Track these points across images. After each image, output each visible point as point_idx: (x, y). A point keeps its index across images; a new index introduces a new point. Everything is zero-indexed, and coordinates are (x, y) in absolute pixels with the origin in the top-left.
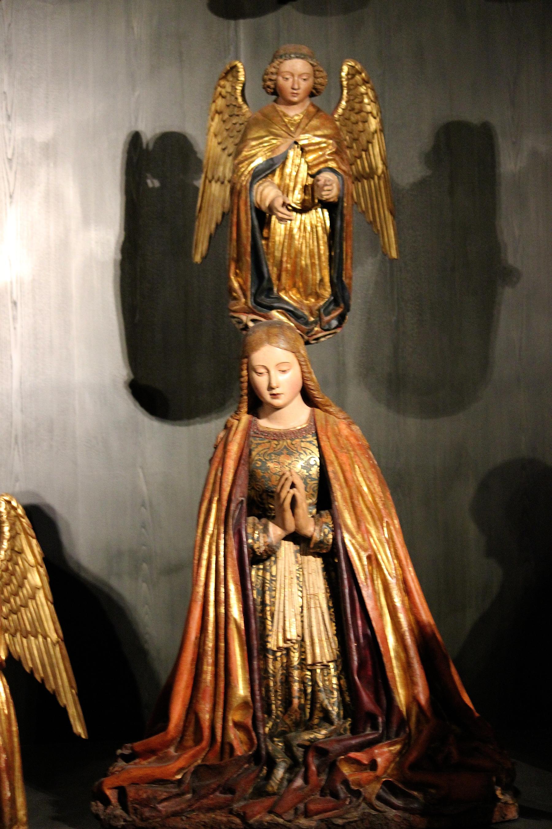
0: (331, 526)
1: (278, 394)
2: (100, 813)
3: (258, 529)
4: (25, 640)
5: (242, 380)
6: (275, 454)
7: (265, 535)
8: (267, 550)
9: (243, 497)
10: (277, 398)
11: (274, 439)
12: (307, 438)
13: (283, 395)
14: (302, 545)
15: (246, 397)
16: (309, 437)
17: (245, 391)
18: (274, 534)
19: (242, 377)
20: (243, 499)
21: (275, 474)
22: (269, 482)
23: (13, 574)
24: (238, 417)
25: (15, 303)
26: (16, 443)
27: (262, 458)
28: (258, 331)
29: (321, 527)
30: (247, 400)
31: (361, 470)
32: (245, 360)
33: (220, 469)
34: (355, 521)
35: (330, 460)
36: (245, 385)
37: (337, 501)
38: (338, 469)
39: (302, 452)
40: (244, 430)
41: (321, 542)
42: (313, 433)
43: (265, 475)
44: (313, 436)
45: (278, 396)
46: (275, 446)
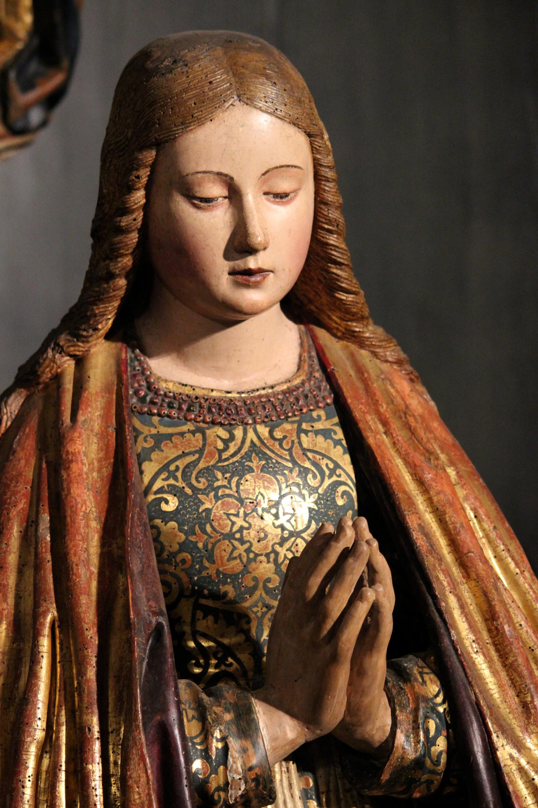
0: (441, 709)
1: (260, 271)
3: (218, 721)
5: (125, 221)
6: (224, 470)
7: (248, 744)
8: (251, 794)
9: (160, 613)
10: (256, 285)
11: (214, 423)
12: (313, 420)
13: (272, 275)
14: (321, 772)
15: (122, 282)
16: (319, 418)
17: (127, 261)
18: (274, 739)
19: (126, 211)
20: (161, 619)
21: (230, 536)
22: (207, 564)
24: (80, 348)
27: (180, 484)
28: (197, 59)
29: (416, 710)
30: (122, 293)
31: (486, 526)
32: (150, 155)
33: (45, 518)
34: (511, 693)
35: (405, 492)
36: (134, 237)
37: (456, 629)
38: (429, 518)
39: (307, 465)
40: (107, 389)
41: (419, 763)
42: (328, 404)
43: (192, 538)
44: (328, 417)
45: (257, 278)
46: (220, 445)
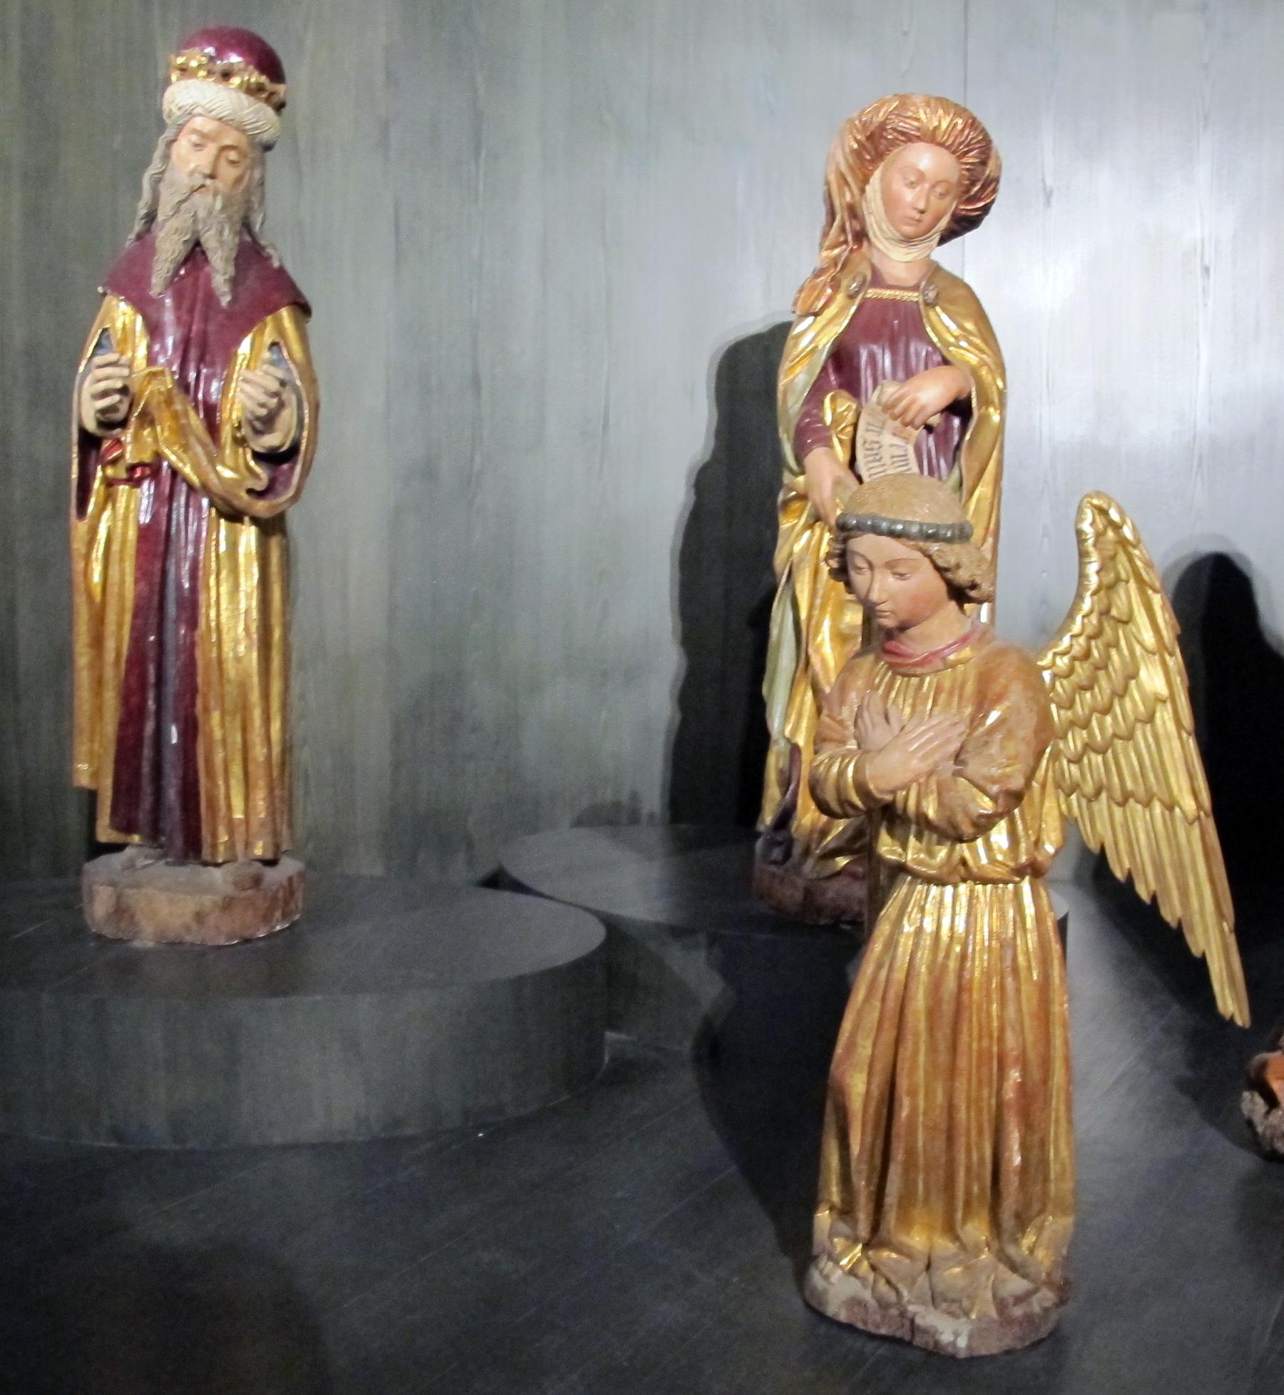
2: (1257, 1118)
4: (1118, 811)
23: (1103, 665)
25: (1206, 270)
26: (1200, 465)
